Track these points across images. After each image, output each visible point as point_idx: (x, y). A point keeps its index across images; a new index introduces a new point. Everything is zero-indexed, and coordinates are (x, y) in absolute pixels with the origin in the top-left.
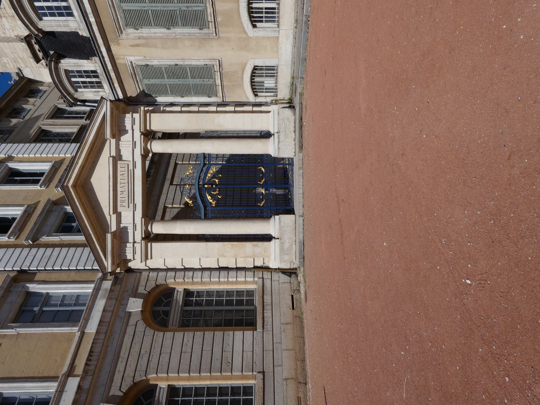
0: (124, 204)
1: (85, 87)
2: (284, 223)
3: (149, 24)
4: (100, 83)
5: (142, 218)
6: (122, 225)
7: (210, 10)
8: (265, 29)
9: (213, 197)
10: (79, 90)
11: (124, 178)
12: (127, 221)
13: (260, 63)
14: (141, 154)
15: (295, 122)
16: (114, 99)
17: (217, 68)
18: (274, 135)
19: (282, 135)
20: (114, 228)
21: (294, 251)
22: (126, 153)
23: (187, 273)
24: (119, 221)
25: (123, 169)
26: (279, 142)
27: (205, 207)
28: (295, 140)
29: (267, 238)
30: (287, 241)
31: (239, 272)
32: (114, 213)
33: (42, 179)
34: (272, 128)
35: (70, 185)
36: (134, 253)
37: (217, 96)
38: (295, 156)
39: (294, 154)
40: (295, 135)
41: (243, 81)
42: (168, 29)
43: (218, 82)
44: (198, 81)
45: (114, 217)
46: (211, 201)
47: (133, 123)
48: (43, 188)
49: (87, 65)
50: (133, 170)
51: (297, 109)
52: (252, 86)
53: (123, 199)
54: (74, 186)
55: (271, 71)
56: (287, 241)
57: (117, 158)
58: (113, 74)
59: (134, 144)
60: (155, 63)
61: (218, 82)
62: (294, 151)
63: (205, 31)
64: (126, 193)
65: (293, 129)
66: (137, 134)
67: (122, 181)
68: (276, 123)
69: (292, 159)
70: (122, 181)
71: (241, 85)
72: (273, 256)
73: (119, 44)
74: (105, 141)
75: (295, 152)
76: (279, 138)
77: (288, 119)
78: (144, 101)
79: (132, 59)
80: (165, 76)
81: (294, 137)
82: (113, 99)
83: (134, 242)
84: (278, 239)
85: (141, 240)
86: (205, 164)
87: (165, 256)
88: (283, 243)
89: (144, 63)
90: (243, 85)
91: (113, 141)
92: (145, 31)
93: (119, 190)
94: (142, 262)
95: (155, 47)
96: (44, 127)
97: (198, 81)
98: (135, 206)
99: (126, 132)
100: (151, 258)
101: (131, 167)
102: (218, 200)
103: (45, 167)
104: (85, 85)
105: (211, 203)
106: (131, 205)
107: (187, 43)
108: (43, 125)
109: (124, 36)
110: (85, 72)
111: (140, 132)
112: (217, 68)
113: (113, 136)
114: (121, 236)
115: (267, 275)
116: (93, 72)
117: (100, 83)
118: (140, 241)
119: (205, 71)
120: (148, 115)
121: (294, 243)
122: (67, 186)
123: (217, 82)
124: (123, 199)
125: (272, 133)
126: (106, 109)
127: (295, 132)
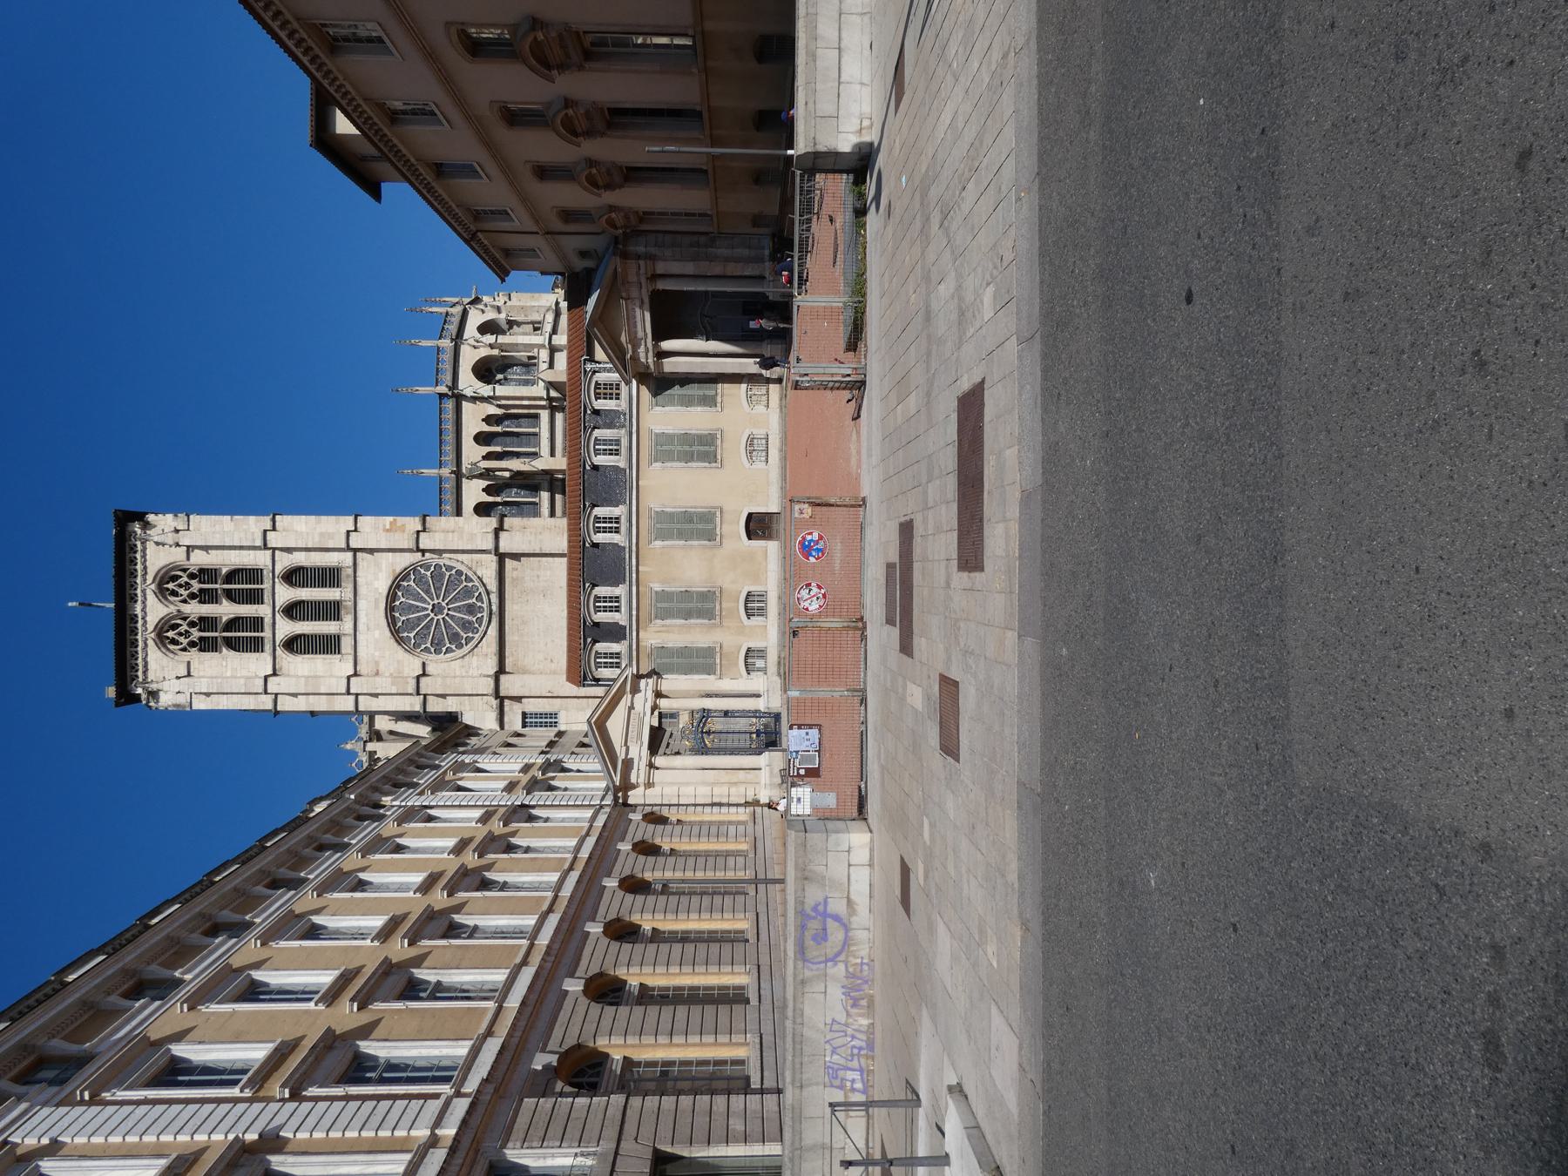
3: (673, 617)
8: (756, 620)
13: (752, 645)
49: (614, 647)
55: (761, 653)
57: (631, 708)
71: (737, 664)
92: (668, 622)
104: (606, 665)
114: (628, 764)
115: (758, 809)
119: (709, 652)
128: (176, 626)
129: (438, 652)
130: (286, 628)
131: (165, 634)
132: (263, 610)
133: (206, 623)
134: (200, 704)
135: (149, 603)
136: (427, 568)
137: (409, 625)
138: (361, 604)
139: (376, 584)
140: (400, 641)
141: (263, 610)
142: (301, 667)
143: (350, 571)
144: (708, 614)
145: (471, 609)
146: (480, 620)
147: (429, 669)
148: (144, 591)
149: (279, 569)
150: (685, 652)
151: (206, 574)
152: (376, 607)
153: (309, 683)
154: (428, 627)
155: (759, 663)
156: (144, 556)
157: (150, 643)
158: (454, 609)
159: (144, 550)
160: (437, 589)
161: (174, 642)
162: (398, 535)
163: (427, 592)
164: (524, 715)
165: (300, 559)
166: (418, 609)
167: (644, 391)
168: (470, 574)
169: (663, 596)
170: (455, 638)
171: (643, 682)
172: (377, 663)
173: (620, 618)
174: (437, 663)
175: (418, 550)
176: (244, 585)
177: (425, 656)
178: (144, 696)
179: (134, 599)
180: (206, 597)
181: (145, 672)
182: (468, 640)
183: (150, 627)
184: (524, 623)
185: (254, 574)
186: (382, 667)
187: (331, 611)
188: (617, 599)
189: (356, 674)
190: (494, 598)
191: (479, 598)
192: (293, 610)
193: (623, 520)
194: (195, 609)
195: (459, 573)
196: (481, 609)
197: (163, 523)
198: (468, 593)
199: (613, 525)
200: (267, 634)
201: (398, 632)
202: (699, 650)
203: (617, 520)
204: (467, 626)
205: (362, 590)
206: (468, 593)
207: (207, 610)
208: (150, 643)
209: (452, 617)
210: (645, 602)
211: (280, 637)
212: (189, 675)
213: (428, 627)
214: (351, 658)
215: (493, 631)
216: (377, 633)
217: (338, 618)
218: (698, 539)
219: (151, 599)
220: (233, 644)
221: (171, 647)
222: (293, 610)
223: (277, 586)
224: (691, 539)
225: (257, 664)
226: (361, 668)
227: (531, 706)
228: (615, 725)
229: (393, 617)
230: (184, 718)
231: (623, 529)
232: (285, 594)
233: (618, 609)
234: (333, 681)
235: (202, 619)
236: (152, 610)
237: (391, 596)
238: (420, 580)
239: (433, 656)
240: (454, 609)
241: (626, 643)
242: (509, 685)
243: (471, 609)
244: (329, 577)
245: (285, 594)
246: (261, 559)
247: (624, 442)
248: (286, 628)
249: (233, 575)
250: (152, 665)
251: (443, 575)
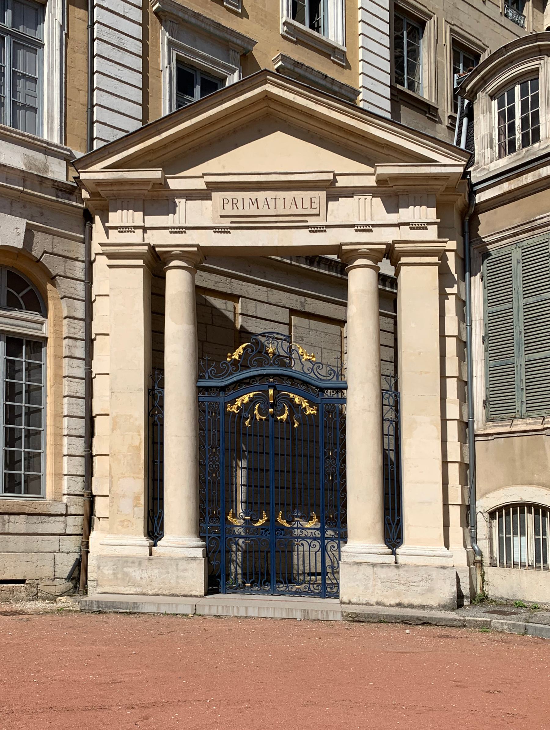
0: (228, 207)
1: (501, 115)
2: (185, 570)
4: (512, 148)
5: (198, 246)
6: (181, 203)
9: (248, 407)
11: (287, 206)
12: (188, 212)
14: (341, 245)
15: (422, 607)
16: (474, 181)
18: (394, 553)
19: (392, 573)
20: (174, 184)
21: (121, 589)
22: (344, 210)
23: (82, 344)
24: (191, 195)
25: (307, 204)
26: (374, 565)
27: (223, 389)
28: (378, 604)
29: (154, 529)
30: (144, 575)
31: (82, 460)
32: (207, 183)
33: (306, 28)
34: (407, 552)
35: (268, 87)
36: (122, 229)
37: (488, 421)
38: (342, 603)
39: (345, 600)
40: (391, 606)
41: (522, 484)
43: (521, 425)
44: (521, 376)
45: (200, 184)
46: (239, 403)
48: (282, 29)
50: (307, 227)
51: (452, 615)
52: (514, 506)
53: (240, 205)
54: (267, 97)
56: (144, 575)
57: (332, 191)
58: (529, 178)
61: (521, 425)
62: (354, 600)
64: (253, 210)
65: (405, 601)
66: (388, 236)
67: (280, 202)
68: (420, 561)
69: (336, 595)
70: (280, 202)
72: (116, 538)
74: (370, 162)
75: (350, 603)
76: (383, 565)
77: (430, 590)
80: (530, 300)
81: (387, 602)
82: (476, 176)
83: (145, 229)
84: (151, 554)
85: (149, 245)
87: (119, 294)
88: (140, 564)
90: (515, 483)
91: (371, 181)
93: (261, 195)
94: (102, 245)
96: (430, 25)
97: (521, 376)
98: (225, 230)
100: (110, 266)
101: (312, 221)
102: (240, 417)
103: (333, 33)
105: (233, 402)
106: (226, 223)
108: (436, 24)
110: (536, 116)
111: (394, 242)
113: (382, 181)
114: (158, 200)
115: (74, 524)
116: (536, 132)
117: (512, 148)
118: (146, 241)
120: (435, 259)
121: (140, 590)
122: (265, 82)
123: (521, 421)
124: (240, 205)
125: (398, 551)
126: (447, 165)
127: (399, 605)
155: (523, 547)
228: (278, 153)
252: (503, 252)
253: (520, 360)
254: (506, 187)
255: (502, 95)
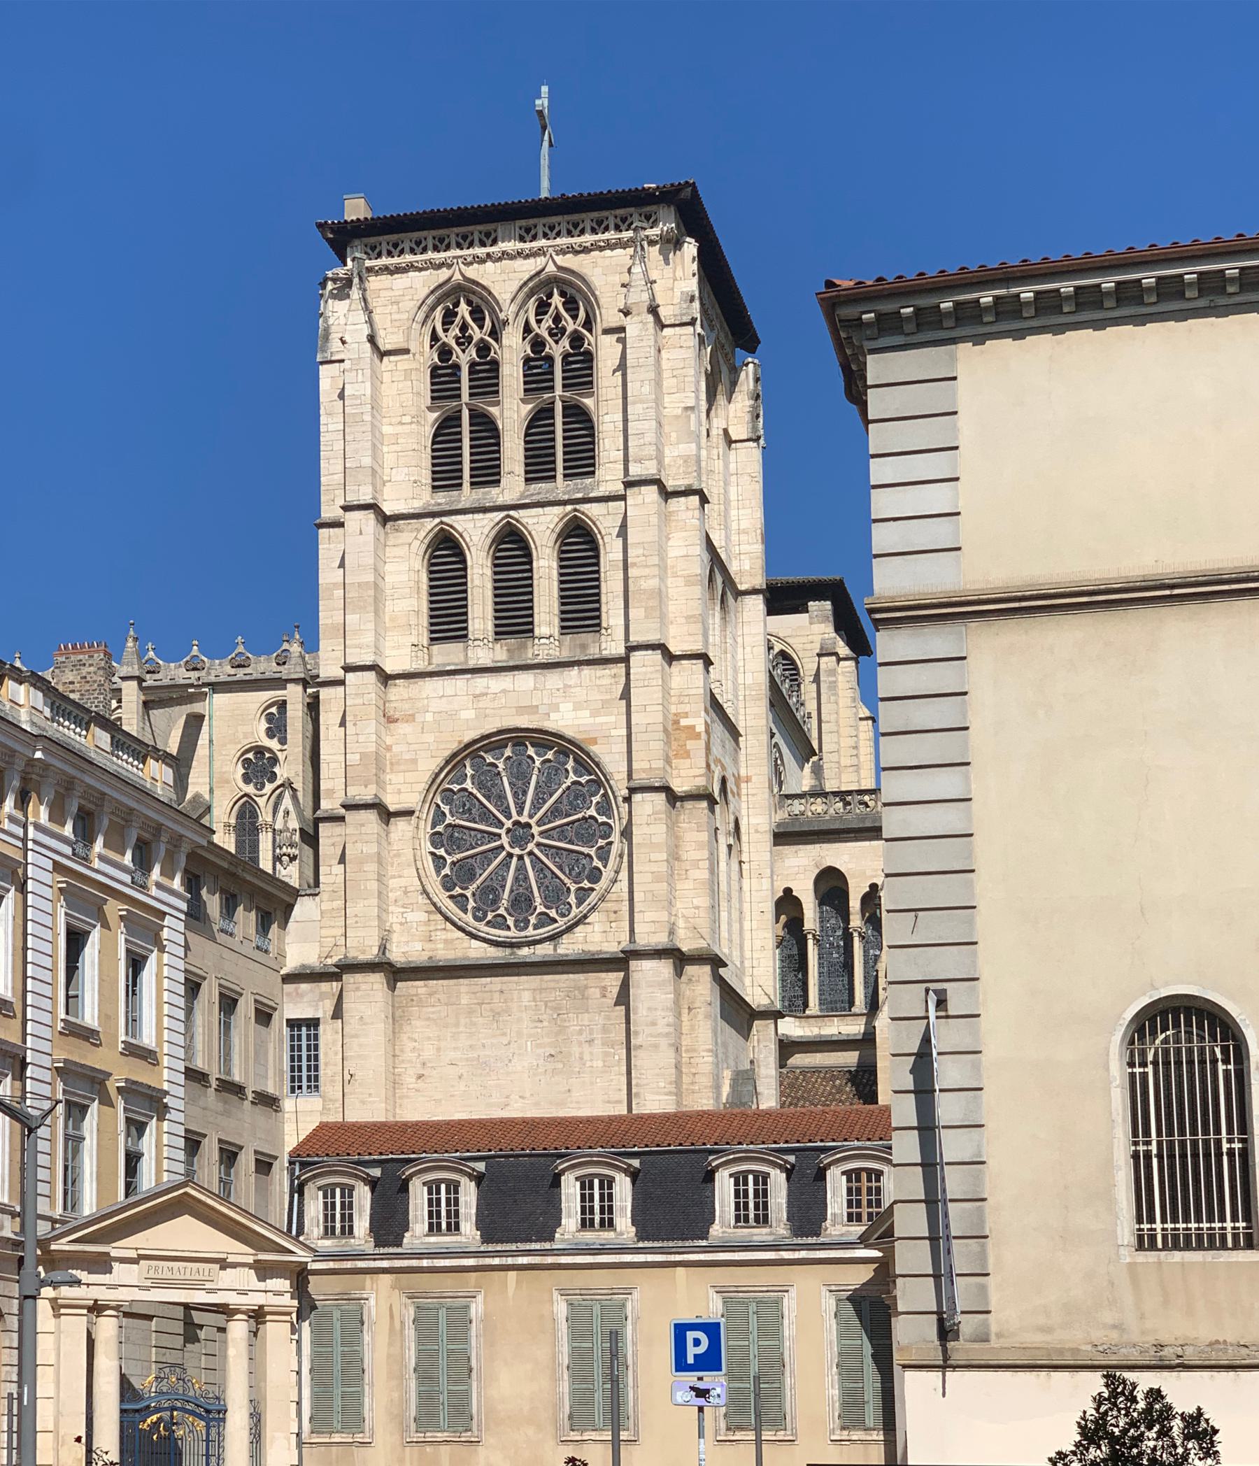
3: (420, 1340)
7: (440, 1436)
10: (321, 1193)
17: (359, 1437)
27: (137, 1411)
42: (415, 1370)
43: (337, 1438)
44: (338, 1402)
47: (278, 1293)
49: (362, 1225)
59: (243, 1293)
60: (367, 1338)
61: (337, 1438)
63: (413, 1426)
73: (393, 1288)
78: (306, 1306)
79: (372, 1302)
86: (208, 1411)
89: (365, 1318)
92: (410, 1332)
95: (390, 1344)
96: (205, 985)
97: (338, 1402)
99: (262, 1278)
102: (151, 1433)
105: (144, 1421)
107: (396, 1395)
108: (210, 985)
109: (404, 1300)
112: (359, 1437)
116: (351, 1227)
119: (353, 1419)
128: (480, 322)
129: (436, 839)
130: (476, 533)
131: (462, 302)
132: (512, 485)
133: (487, 375)
134: (328, 378)
135: (519, 262)
136: (605, 808)
137: (488, 778)
138: (525, 680)
139: (566, 707)
140: (455, 762)
141: (512, 485)
142: (406, 568)
143: (593, 652)
144: (426, 1418)
145: (522, 903)
146: (499, 923)
147: (400, 827)
148: (540, 252)
149: (593, 510)
150: (354, 1370)
151: (581, 367)
152: (521, 710)
153: (370, 588)
154: (486, 816)
156: (610, 246)
157: (444, 274)
158: (521, 869)
159: (622, 245)
160: (561, 832)
161: (449, 317)
162: (657, 746)
163: (555, 812)
164: (313, 1023)
165: (611, 552)
166: (520, 794)
167: (864, 1274)
168: (593, 898)
169: (460, 1321)
170: (464, 873)
171: (283, 1284)
172: (410, 718)
173: (417, 1234)
174: (410, 842)
175: (632, 790)
176: (564, 442)
177: (427, 815)
178: (341, 272)
179: (527, 234)
180: (537, 372)
181: (386, 270)
182: (460, 901)
183: (473, 272)
184: (496, 1015)
185: (583, 460)
186: (403, 728)
187: (514, 619)
188: (454, 1227)
189: (386, 678)
190: (544, 951)
191: (545, 920)
192: (512, 545)
193: (607, 1236)
194: (512, 352)
195: (595, 875)
196: (522, 924)
197: (678, 277)
198: (555, 896)
199: (597, 1215)
200: (467, 495)
201: (474, 755)
202: (359, 1396)
203: (608, 1224)
204: (489, 895)
205: (554, 679)
206: (555, 896)
207: (512, 375)
208: (444, 274)
209: (505, 864)
210: (447, 1284)
211: (460, 524)
212: (383, 354)
213: (486, 816)
214: (421, 666)
215: (478, 951)
216: (469, 714)
217: (502, 632)
218: (573, 1392)
219: (528, 267)
220: (446, 430)
221: (439, 314)
222: (512, 545)
223: (558, 510)
224: (574, 1378)
225: (406, 482)
226: (399, 690)
227: (328, 1034)
229: (502, 745)
230: (305, 349)
231: (590, 1237)
232: (542, 528)
233: (434, 1228)
234: (369, 638)
235: (495, 365)
236: (504, 272)
237: (545, 739)
238: (577, 796)
239: (426, 830)
240: (521, 869)
241: (369, 1247)
242: (367, 993)
243: (522, 903)
244: (581, 610)
245: (542, 528)
246: (608, 477)
247: (760, 1234)
248: (476, 533)
249: (580, 419)
250: (401, 281)
251: (589, 842)
252: (326, 1309)
253: (338, 1391)
254: (331, 1265)
255: (328, 1191)
